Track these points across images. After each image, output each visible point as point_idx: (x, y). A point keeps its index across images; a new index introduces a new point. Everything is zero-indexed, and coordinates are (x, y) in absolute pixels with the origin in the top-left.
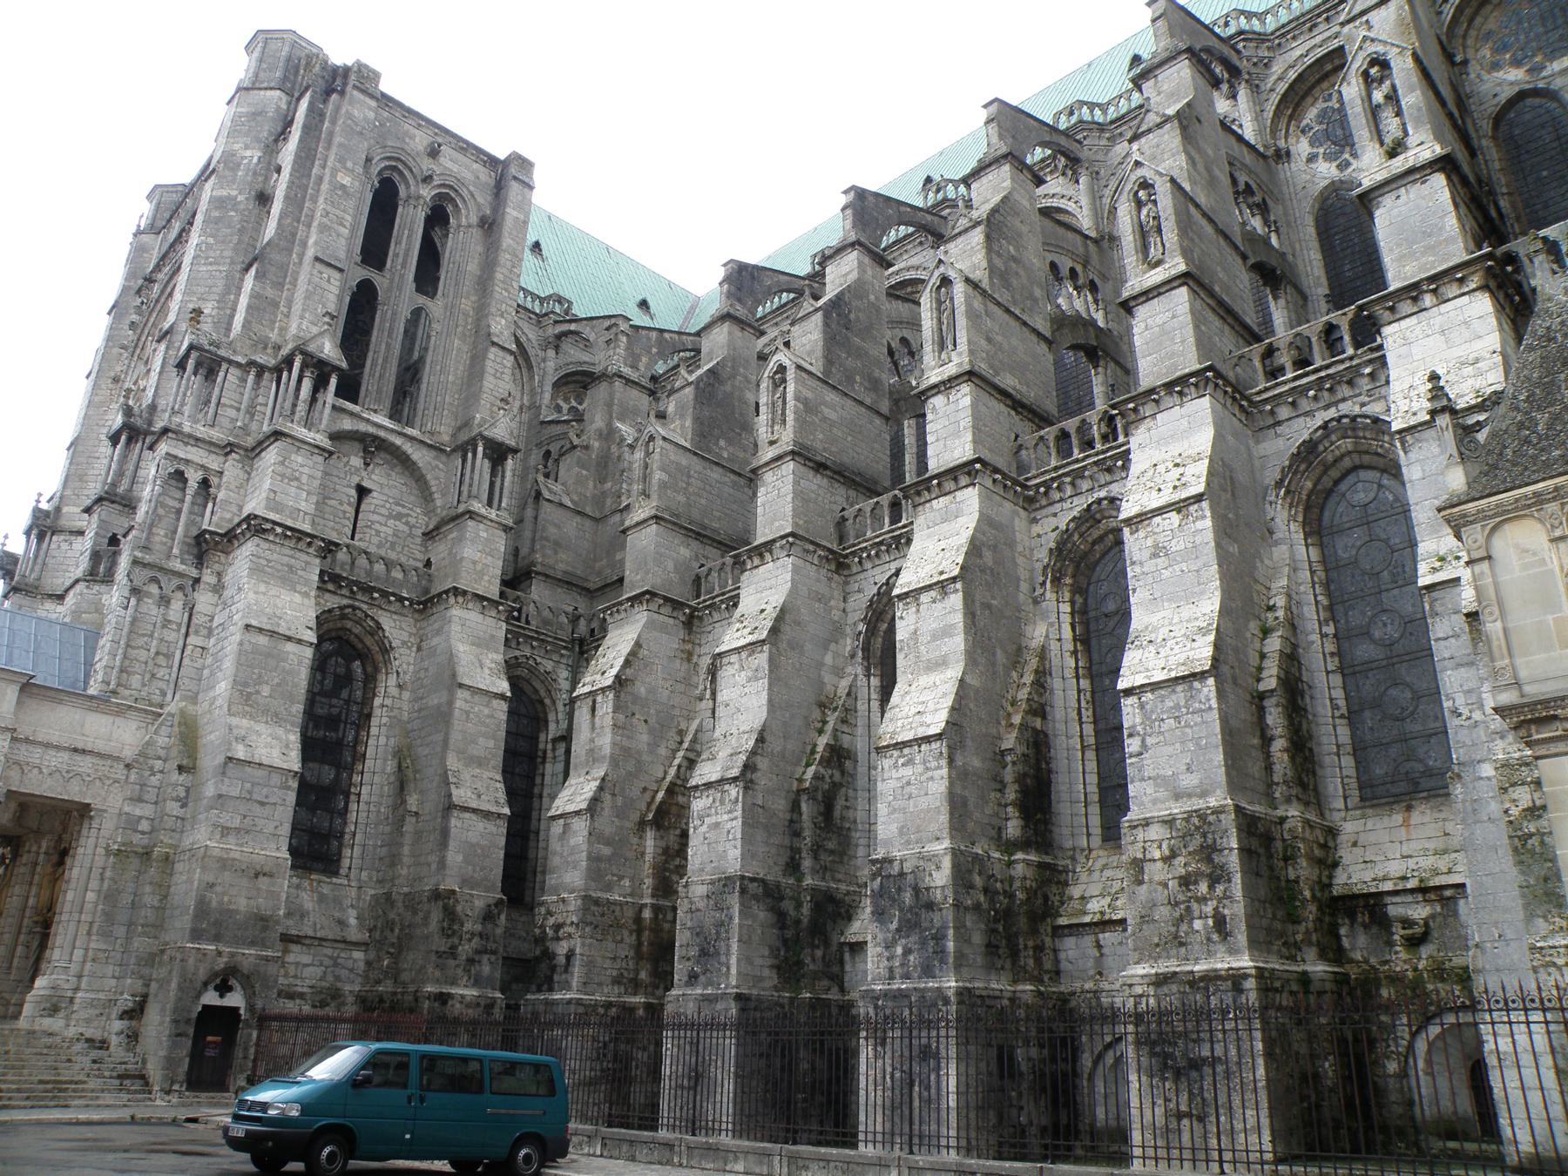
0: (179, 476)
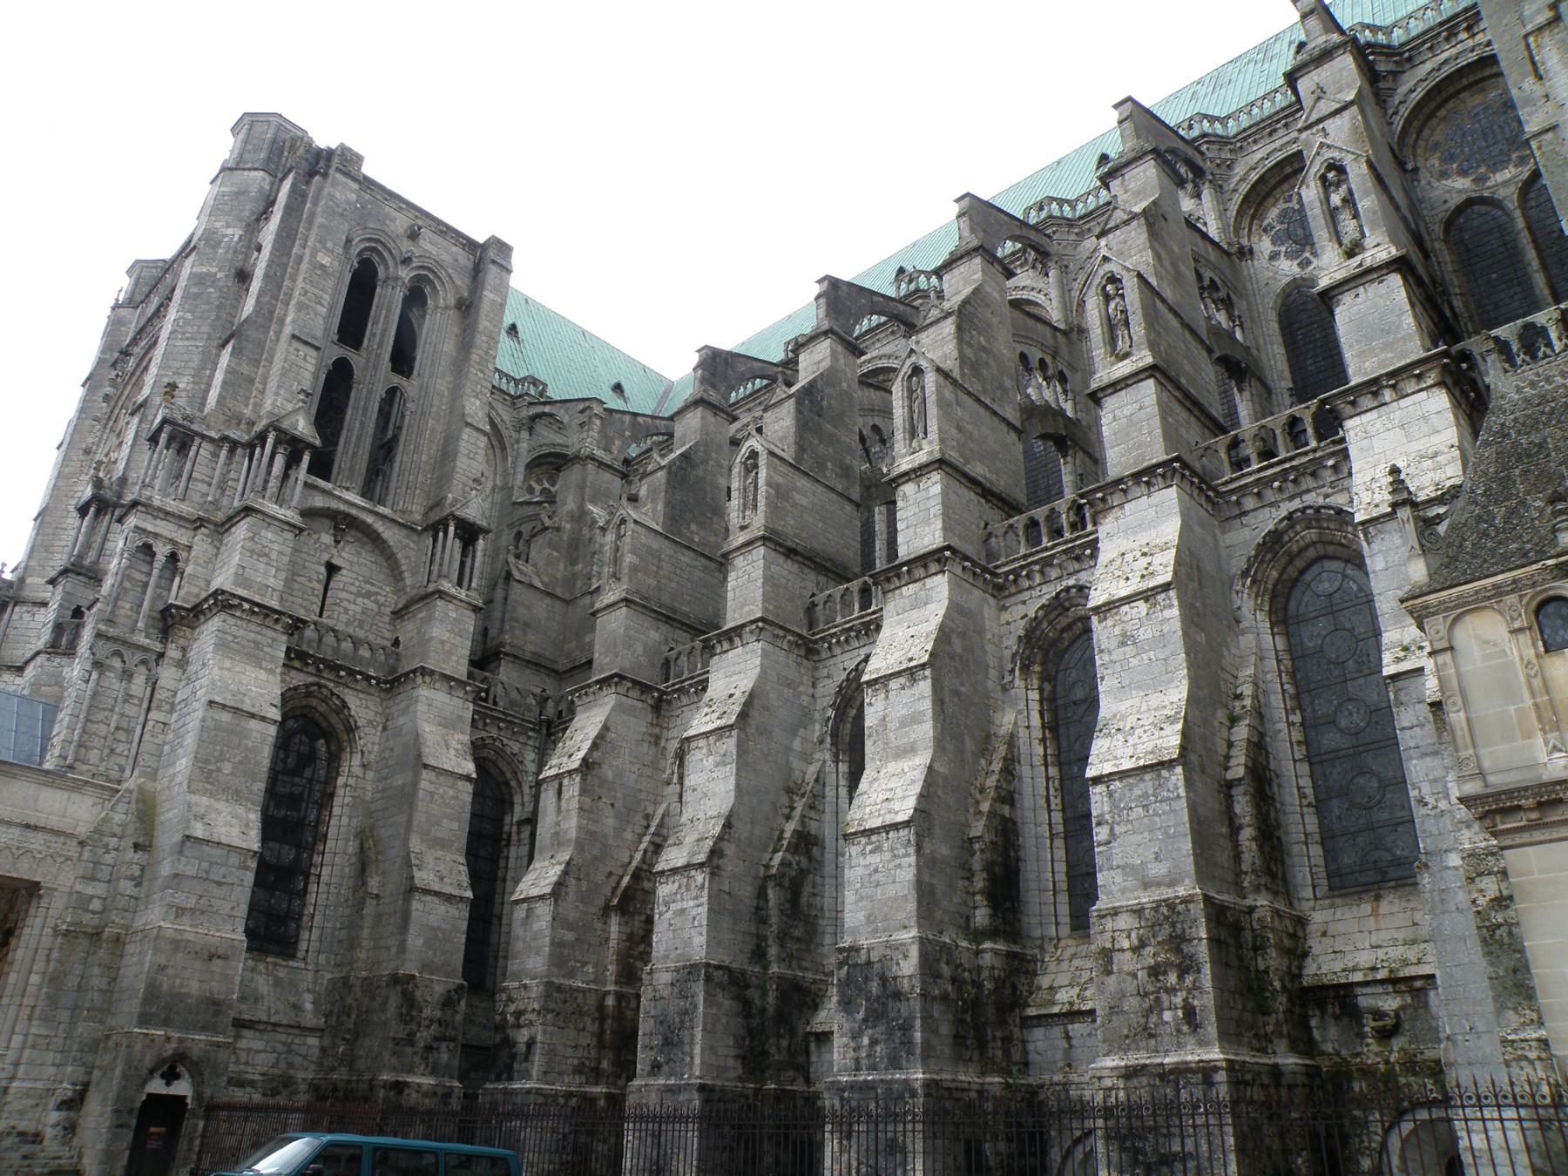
0: (147, 550)
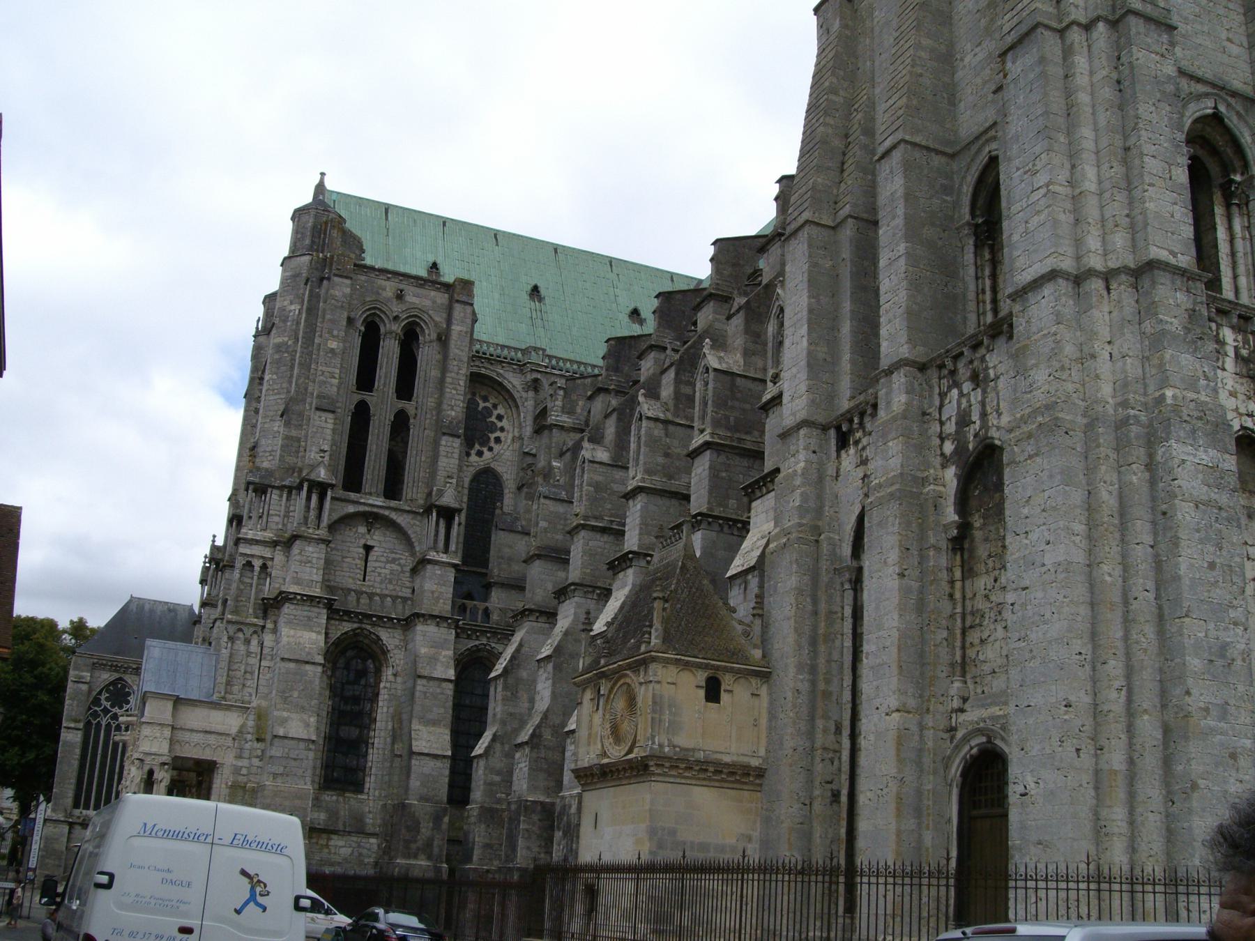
0: (249, 565)
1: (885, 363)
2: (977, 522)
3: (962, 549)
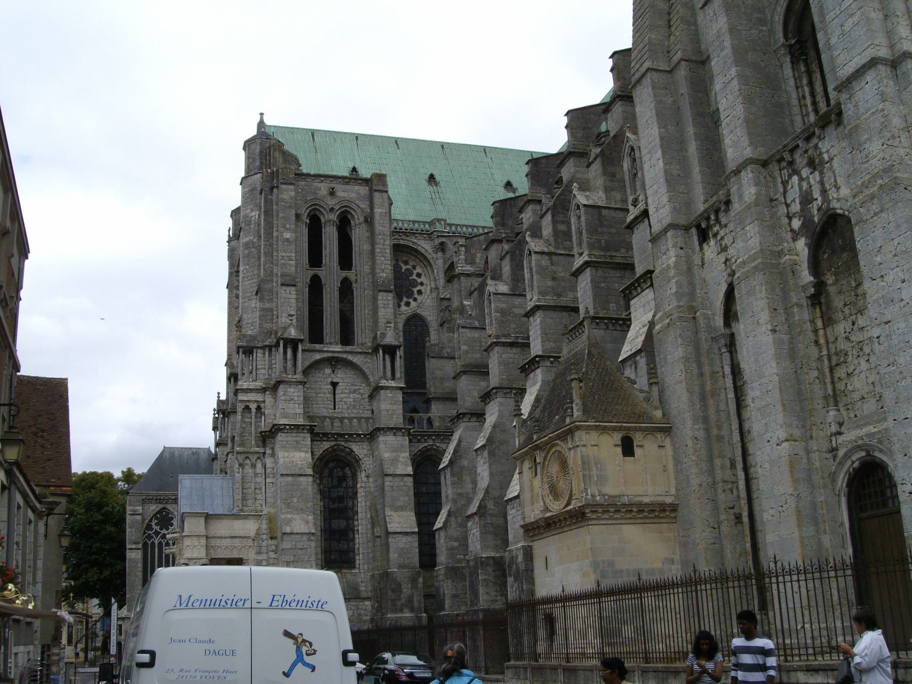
0: (247, 408)
1: (731, 165)
2: (830, 279)
3: (820, 304)
